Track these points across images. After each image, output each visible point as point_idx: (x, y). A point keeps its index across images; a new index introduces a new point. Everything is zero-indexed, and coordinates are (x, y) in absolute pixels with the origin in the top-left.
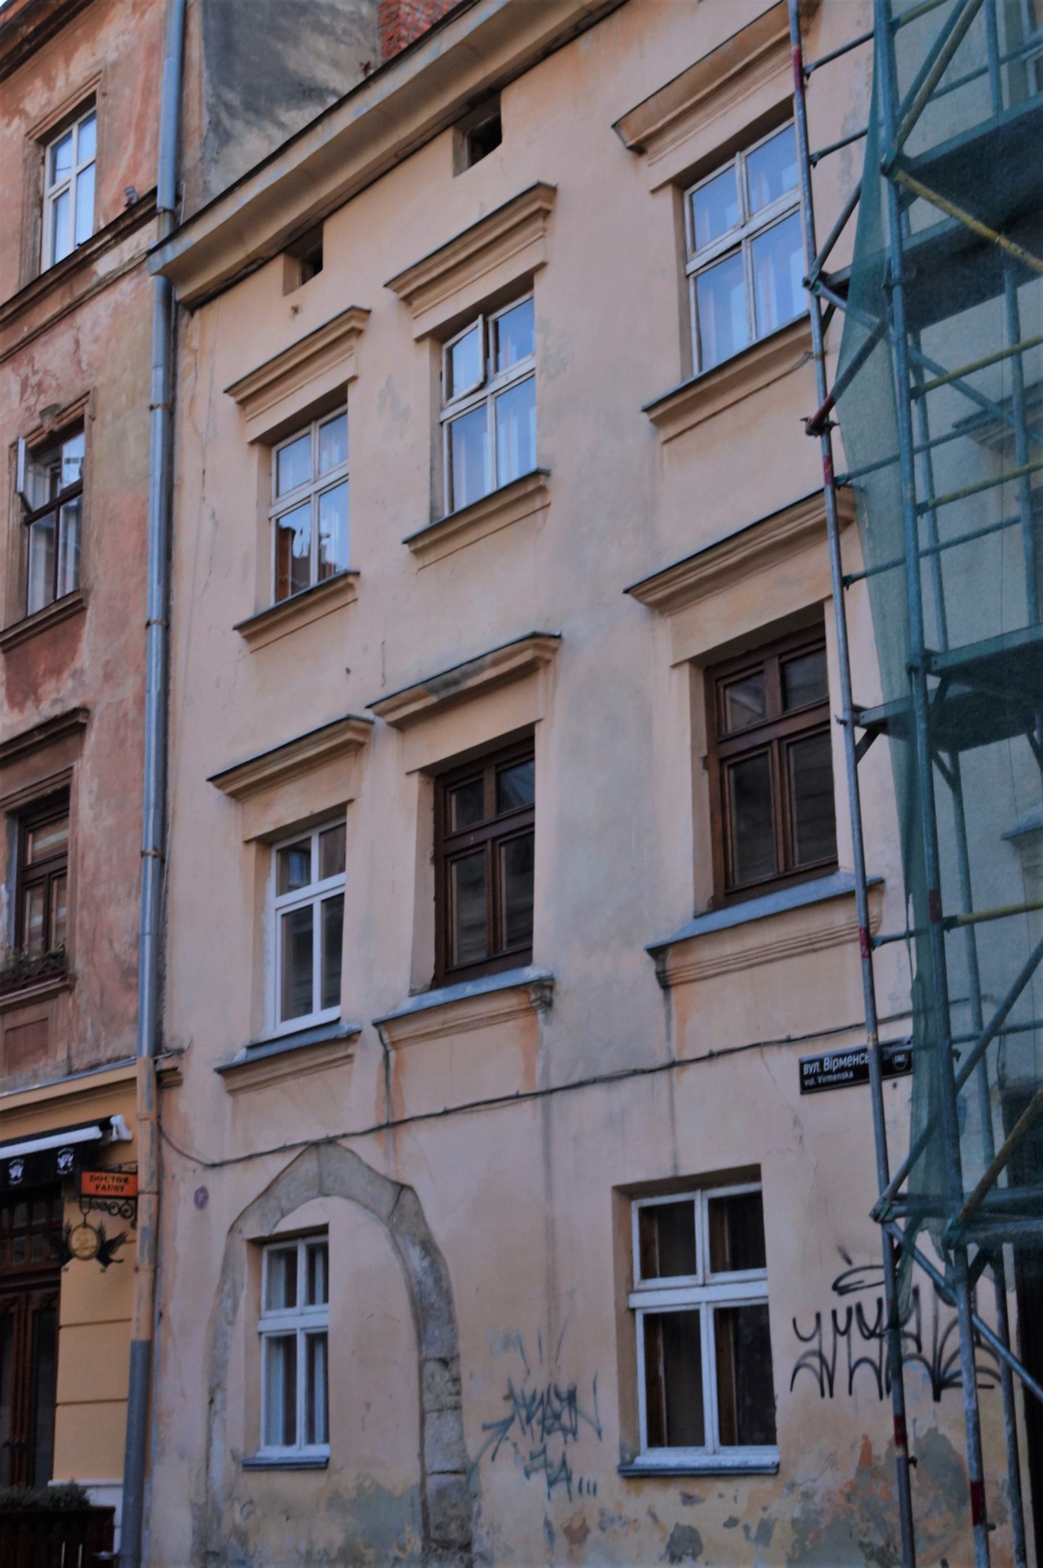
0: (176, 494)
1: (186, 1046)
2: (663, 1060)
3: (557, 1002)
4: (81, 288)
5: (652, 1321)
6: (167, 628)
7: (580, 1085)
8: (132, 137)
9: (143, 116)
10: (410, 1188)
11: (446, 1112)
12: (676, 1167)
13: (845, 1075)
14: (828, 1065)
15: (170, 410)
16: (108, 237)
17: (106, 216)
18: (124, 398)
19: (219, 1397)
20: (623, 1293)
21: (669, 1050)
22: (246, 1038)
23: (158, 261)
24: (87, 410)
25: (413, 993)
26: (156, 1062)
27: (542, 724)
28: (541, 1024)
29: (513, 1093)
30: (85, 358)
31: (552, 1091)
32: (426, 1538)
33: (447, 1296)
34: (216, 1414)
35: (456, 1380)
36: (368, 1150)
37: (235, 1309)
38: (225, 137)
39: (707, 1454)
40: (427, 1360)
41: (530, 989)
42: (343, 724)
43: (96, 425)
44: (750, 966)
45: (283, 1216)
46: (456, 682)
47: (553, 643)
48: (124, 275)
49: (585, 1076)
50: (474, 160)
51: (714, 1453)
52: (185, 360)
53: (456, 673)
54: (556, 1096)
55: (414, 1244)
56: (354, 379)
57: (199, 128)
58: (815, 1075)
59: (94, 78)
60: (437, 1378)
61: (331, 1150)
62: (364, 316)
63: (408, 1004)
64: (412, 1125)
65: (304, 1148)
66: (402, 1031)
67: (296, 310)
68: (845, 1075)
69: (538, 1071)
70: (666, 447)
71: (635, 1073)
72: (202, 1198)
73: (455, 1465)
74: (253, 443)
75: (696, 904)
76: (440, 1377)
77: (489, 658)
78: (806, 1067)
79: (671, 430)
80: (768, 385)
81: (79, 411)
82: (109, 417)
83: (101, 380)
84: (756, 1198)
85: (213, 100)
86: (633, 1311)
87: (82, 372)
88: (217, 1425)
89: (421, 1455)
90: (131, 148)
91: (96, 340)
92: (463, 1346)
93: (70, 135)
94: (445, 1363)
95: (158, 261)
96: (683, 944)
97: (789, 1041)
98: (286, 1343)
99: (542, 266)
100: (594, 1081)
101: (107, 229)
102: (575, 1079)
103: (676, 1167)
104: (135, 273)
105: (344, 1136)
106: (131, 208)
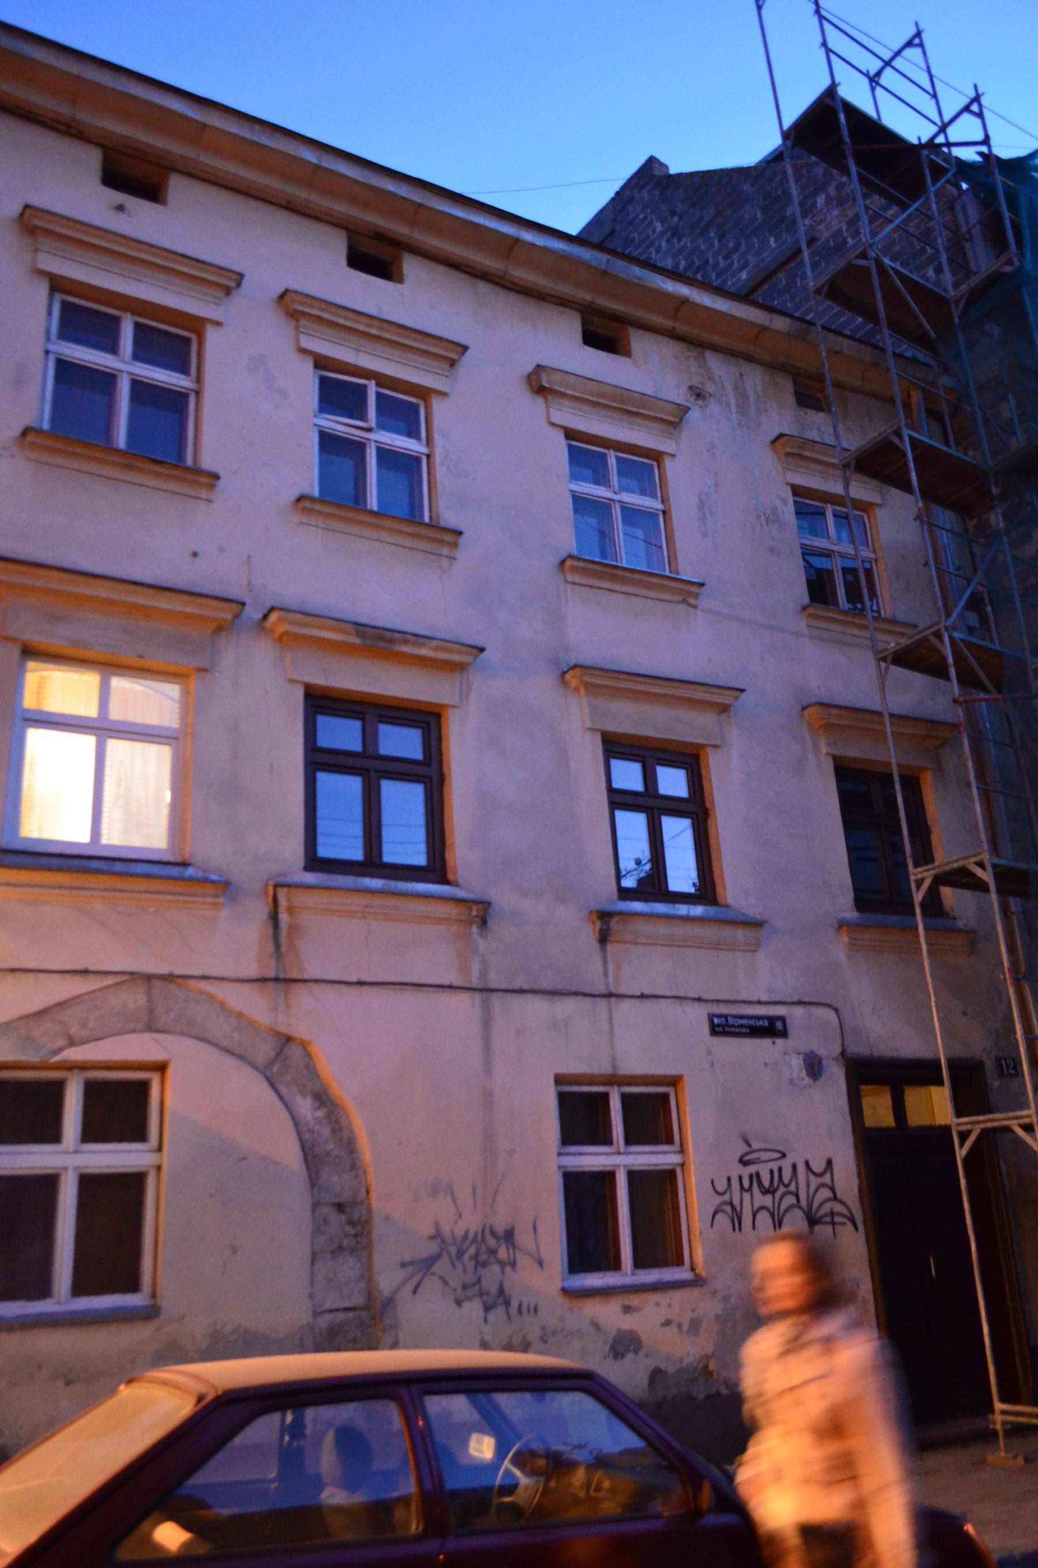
2: (601, 989)
7: (521, 991)
13: (744, 1030)
14: (731, 1021)
31: (492, 991)
49: (527, 987)
54: (494, 995)
58: (723, 1026)
64: (316, 988)
68: (744, 1030)
97: (700, 1000)
102: (517, 985)
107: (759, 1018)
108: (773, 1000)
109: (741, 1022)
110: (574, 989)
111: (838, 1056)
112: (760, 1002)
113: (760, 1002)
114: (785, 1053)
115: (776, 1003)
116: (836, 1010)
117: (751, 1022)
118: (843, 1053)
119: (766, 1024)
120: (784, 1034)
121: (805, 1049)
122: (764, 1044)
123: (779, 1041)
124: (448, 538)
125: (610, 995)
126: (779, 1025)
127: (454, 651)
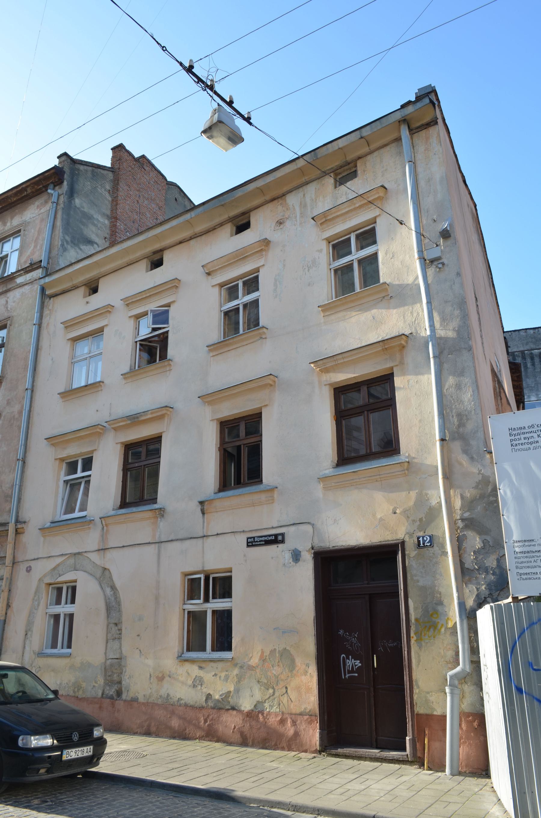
0: (39, 351)
1: (27, 521)
2: (201, 534)
3: (165, 515)
4: (10, 286)
5: (189, 612)
6: (32, 391)
7: (172, 540)
8: (33, 244)
9: (37, 238)
10: (109, 570)
11: (124, 547)
12: (203, 567)
13: (262, 543)
14: (256, 539)
15: (40, 325)
16: (22, 272)
17: (21, 266)
18: (23, 321)
19: (29, 633)
20: (182, 604)
21: (203, 532)
22: (50, 519)
23: (42, 282)
24: (9, 323)
25: (113, 510)
26: (16, 525)
27: (165, 433)
28: (159, 522)
29: (148, 542)
30: (9, 307)
31: (162, 542)
32: (105, 680)
33: (119, 603)
34: (28, 638)
35: (120, 630)
36: (95, 557)
37: (38, 605)
38: (65, 250)
39: (207, 654)
40: (110, 623)
41: (157, 511)
42: (96, 426)
43: (12, 327)
44: (232, 509)
45: (60, 576)
46: (137, 418)
47: (171, 410)
48: (27, 284)
49: (174, 538)
50: (152, 269)
51: (209, 653)
52: (46, 312)
53: (138, 415)
54: (163, 544)
55: (108, 587)
56: (107, 325)
57: (58, 245)
58: (252, 542)
59: (21, 225)
60: (113, 629)
61: (80, 556)
62: (112, 307)
63: (113, 513)
64: (111, 550)
65: (70, 555)
66: (109, 521)
67: (87, 303)
68: (262, 543)
69: (157, 536)
70: (212, 358)
71: (191, 538)
72: (29, 570)
73: (118, 656)
74: (68, 340)
75: (214, 490)
76: (114, 629)
77: (150, 412)
78: (249, 540)
79: (214, 353)
80: (247, 345)
81: (5, 323)
82: (17, 325)
83: (14, 314)
84: (230, 578)
85: (62, 238)
86: (184, 610)
87: (8, 310)
88: (27, 642)
89: (105, 653)
90: (32, 247)
91: (14, 302)
92: (124, 619)
93: (10, 240)
94: (116, 624)
95: (42, 282)
96: (211, 501)
97: (244, 531)
98: (56, 617)
99: (174, 302)
100: (177, 540)
101: (22, 270)
102: (170, 539)
103: (203, 567)
104: (30, 284)
105: (86, 552)
106: (31, 264)
107: (270, 536)
108: (280, 525)
109: (261, 539)
110: (190, 536)
111: (309, 549)
112: (273, 528)
113: (273, 528)
114: (282, 551)
115: (281, 527)
117: (266, 538)
118: (313, 548)
119: (273, 538)
120: (283, 541)
121: (293, 548)
122: (273, 548)
123: (280, 546)
125: (205, 536)
126: (280, 538)
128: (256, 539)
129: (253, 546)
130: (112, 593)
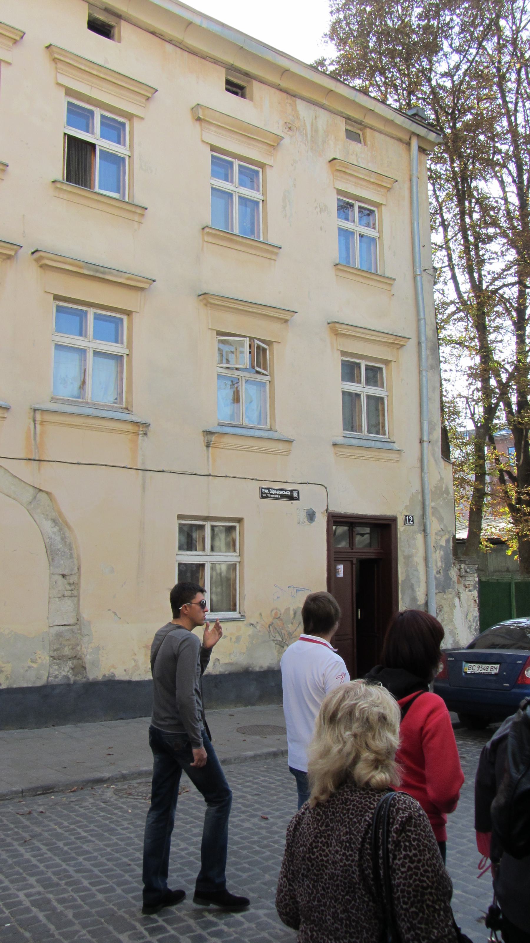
13: (277, 496)
14: (271, 491)
58: (267, 494)
68: (277, 496)
97: (256, 480)
107: (286, 490)
109: (276, 492)
116: (326, 488)
117: (282, 493)
118: (327, 510)
119: (289, 494)
120: (297, 499)
123: (295, 502)
124: (139, 211)
126: (295, 495)
127: (142, 282)
128: (271, 490)
129: (267, 497)
130: (56, 529)
